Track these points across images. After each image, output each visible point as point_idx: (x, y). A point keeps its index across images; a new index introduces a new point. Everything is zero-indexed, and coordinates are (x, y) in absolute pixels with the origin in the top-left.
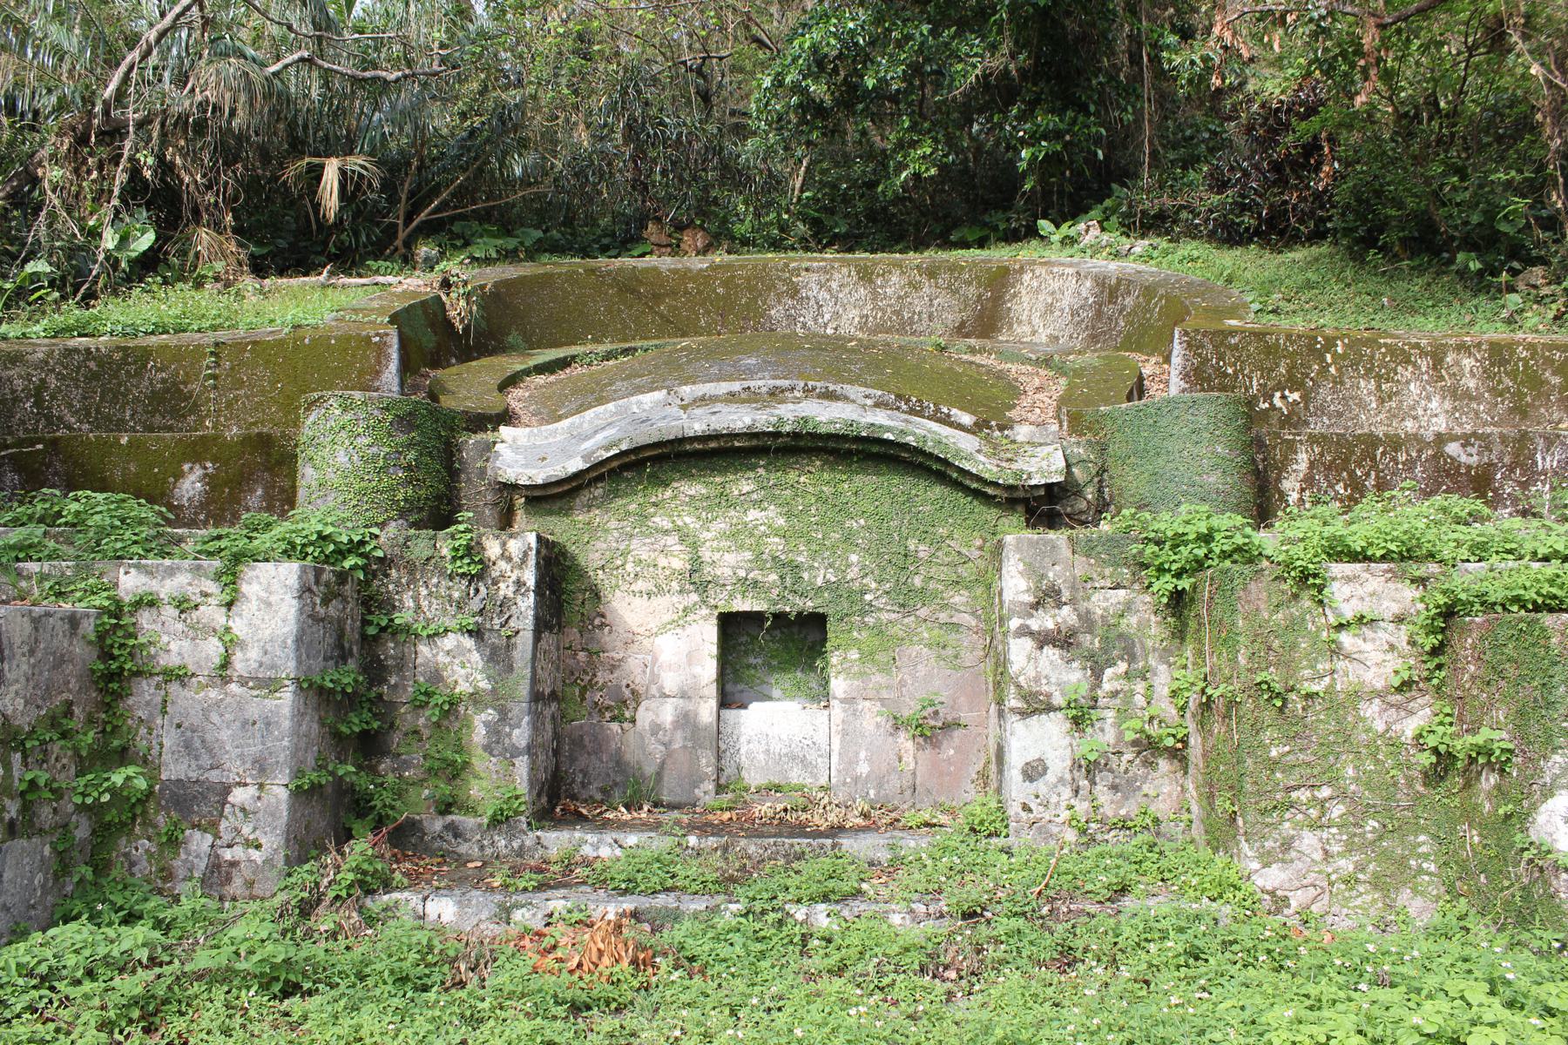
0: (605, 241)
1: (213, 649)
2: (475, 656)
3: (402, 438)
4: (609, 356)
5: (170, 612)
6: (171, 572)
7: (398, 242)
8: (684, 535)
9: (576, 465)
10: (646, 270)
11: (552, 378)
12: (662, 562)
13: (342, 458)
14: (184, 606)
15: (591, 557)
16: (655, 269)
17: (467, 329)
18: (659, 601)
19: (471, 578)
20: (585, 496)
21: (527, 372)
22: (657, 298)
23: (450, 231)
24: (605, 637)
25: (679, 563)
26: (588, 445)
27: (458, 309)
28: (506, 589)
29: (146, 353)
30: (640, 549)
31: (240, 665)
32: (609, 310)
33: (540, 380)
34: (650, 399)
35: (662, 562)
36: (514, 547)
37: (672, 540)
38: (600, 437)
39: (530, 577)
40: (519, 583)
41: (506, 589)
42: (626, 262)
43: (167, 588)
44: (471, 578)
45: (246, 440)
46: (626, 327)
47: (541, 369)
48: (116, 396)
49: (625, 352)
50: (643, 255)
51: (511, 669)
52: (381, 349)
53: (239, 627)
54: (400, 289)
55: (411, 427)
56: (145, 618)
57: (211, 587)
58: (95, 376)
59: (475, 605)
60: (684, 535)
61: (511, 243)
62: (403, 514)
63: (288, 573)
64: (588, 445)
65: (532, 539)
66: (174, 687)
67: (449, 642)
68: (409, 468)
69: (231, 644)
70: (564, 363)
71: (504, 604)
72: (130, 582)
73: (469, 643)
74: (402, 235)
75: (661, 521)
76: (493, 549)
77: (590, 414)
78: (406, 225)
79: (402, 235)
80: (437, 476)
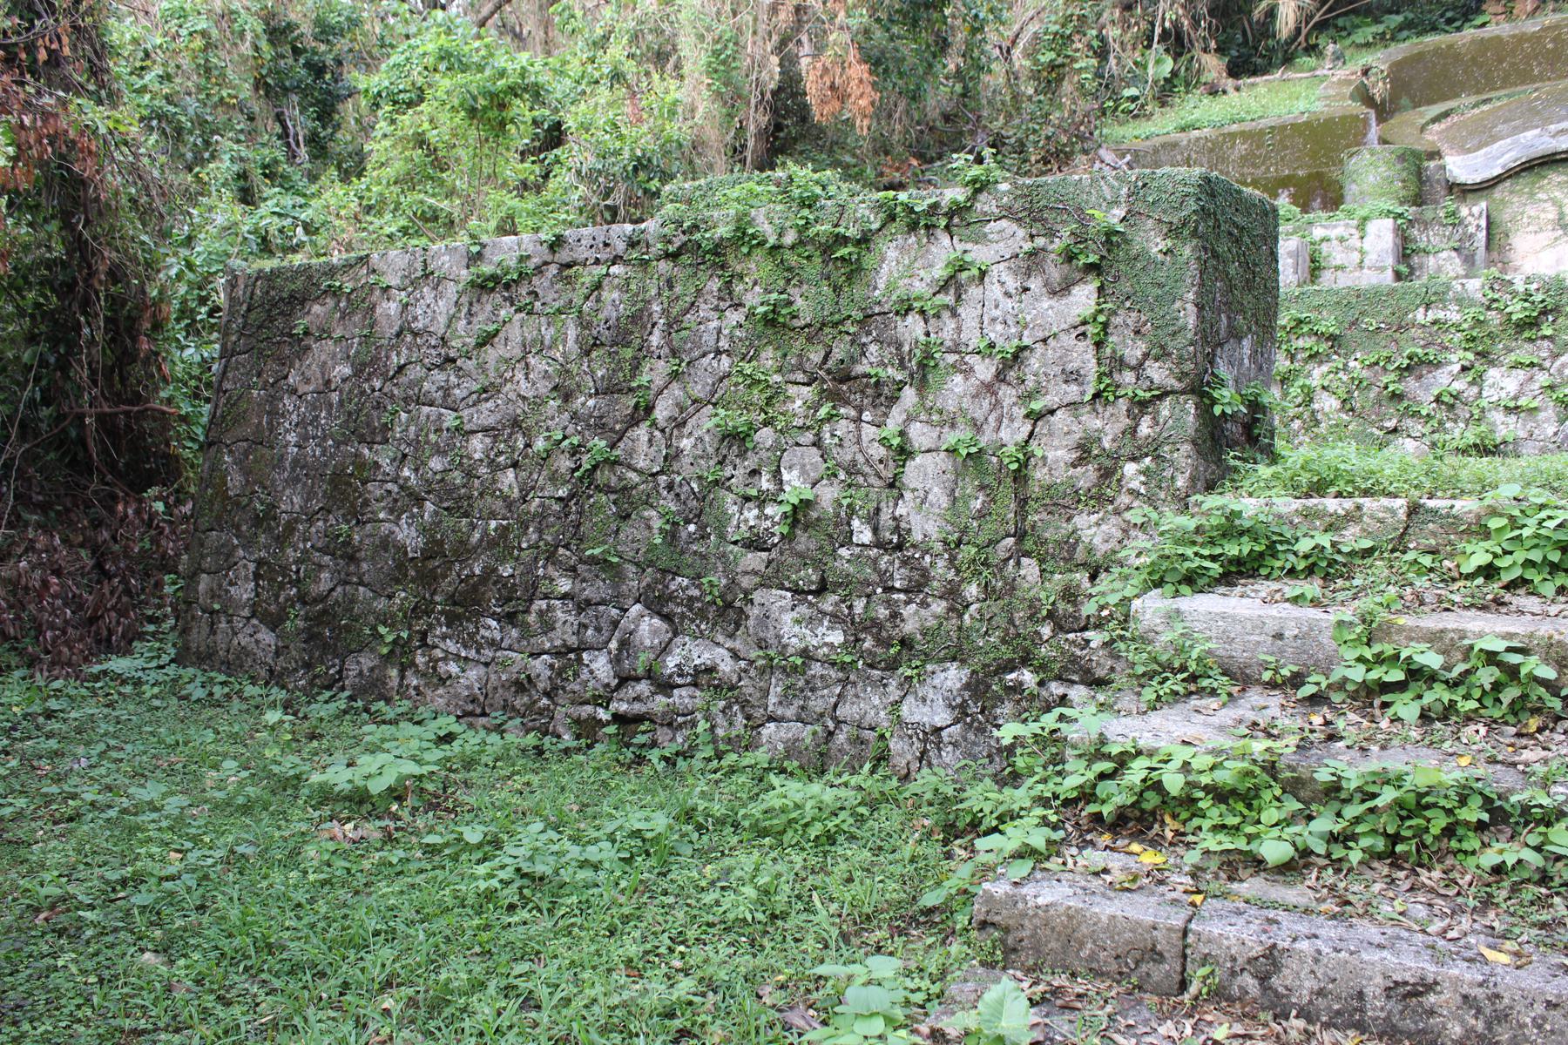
0: (1449, 14)
1: (1356, 256)
2: (1457, 260)
3: (1399, 167)
4: (1476, 106)
5: (1335, 242)
6: (1335, 227)
7: (1301, 38)
8: (1554, 201)
9: (1497, 171)
10: (1491, 39)
11: (1443, 126)
12: (1543, 216)
13: (1371, 179)
14: (1342, 240)
15: (1505, 216)
16: (1498, 37)
17: (1383, 101)
18: (1541, 236)
19: (1454, 225)
20: (1500, 187)
21: (1427, 124)
22: (1501, 61)
23: (1336, 26)
24: (1512, 255)
25: (1552, 214)
26: (1501, 161)
27: (1379, 90)
28: (1471, 229)
29: (1232, 136)
30: (1531, 211)
31: (1367, 262)
32: (1465, 72)
33: (1436, 127)
34: (1530, 134)
35: (1543, 216)
36: (1475, 210)
37: (1548, 205)
38: (1507, 156)
39: (1483, 223)
40: (1478, 226)
41: (1471, 229)
42: (1469, 33)
43: (1333, 233)
44: (1454, 225)
45: (1310, 175)
46: (1478, 82)
47: (1435, 120)
48: (1224, 160)
49: (1485, 102)
50: (1484, 25)
51: (1473, 264)
52: (1366, 121)
53: (1366, 247)
54: (1335, 79)
55: (1404, 160)
56: (1324, 247)
57: (1354, 231)
58: (1211, 150)
59: (1457, 237)
60: (1554, 201)
61: (1380, 28)
62: (1402, 203)
63: (1389, 223)
64: (1501, 161)
65: (1483, 205)
66: (1339, 273)
67: (1444, 255)
68: (1404, 181)
69: (1362, 252)
70: (1446, 115)
71: (1471, 236)
72: (1318, 233)
73: (1454, 254)
74: (1304, 32)
75: (1542, 196)
76: (1464, 211)
77: (1496, 146)
78: (1307, 23)
79: (1304, 32)
80: (1422, 186)
